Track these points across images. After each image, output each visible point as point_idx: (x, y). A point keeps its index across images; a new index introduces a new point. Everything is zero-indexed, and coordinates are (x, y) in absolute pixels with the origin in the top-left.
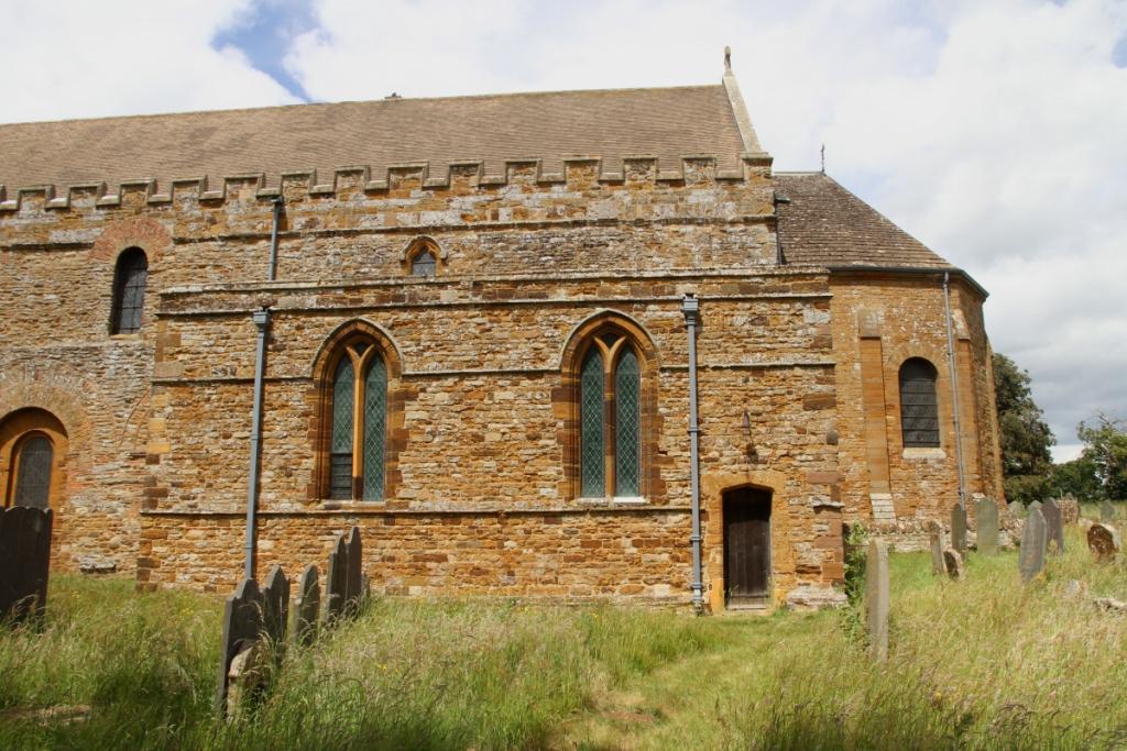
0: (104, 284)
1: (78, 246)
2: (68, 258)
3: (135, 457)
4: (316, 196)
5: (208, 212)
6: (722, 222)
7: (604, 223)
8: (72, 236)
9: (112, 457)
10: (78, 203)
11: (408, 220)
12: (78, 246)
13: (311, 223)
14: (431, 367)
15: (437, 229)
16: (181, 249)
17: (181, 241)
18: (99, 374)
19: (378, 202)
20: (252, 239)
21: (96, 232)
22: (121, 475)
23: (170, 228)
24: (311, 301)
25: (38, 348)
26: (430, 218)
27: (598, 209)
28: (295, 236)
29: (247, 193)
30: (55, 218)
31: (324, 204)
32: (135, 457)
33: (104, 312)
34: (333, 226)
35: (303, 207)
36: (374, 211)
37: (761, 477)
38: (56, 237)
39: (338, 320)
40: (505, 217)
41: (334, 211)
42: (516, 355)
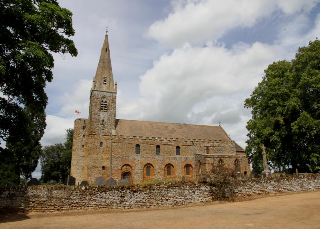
0: (175, 149)
1: (172, 145)
2: (170, 146)
3: (182, 169)
4: (196, 142)
5: (185, 142)
6: (231, 147)
7: (223, 147)
8: (171, 144)
9: (179, 169)
10: (171, 140)
11: (206, 145)
12: (172, 145)
13: (196, 145)
14: (226, 162)
15: (209, 146)
16: (183, 146)
17: (183, 145)
18: (176, 160)
19: (203, 143)
20: (191, 146)
21: (173, 143)
22: (180, 171)
23: (182, 144)
24: (217, 157)
25: (169, 157)
26: (208, 145)
27: (222, 145)
28: (195, 146)
29: (189, 140)
30: (168, 141)
31: (197, 143)
32: (182, 169)
33: (176, 153)
34: (199, 145)
35: (195, 143)
36: (202, 144)
37: (246, 171)
38: (169, 144)
39: (219, 158)
40: (214, 146)
41: (199, 143)
42: (231, 162)
